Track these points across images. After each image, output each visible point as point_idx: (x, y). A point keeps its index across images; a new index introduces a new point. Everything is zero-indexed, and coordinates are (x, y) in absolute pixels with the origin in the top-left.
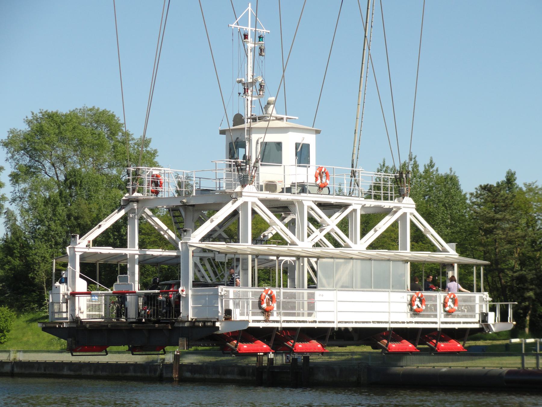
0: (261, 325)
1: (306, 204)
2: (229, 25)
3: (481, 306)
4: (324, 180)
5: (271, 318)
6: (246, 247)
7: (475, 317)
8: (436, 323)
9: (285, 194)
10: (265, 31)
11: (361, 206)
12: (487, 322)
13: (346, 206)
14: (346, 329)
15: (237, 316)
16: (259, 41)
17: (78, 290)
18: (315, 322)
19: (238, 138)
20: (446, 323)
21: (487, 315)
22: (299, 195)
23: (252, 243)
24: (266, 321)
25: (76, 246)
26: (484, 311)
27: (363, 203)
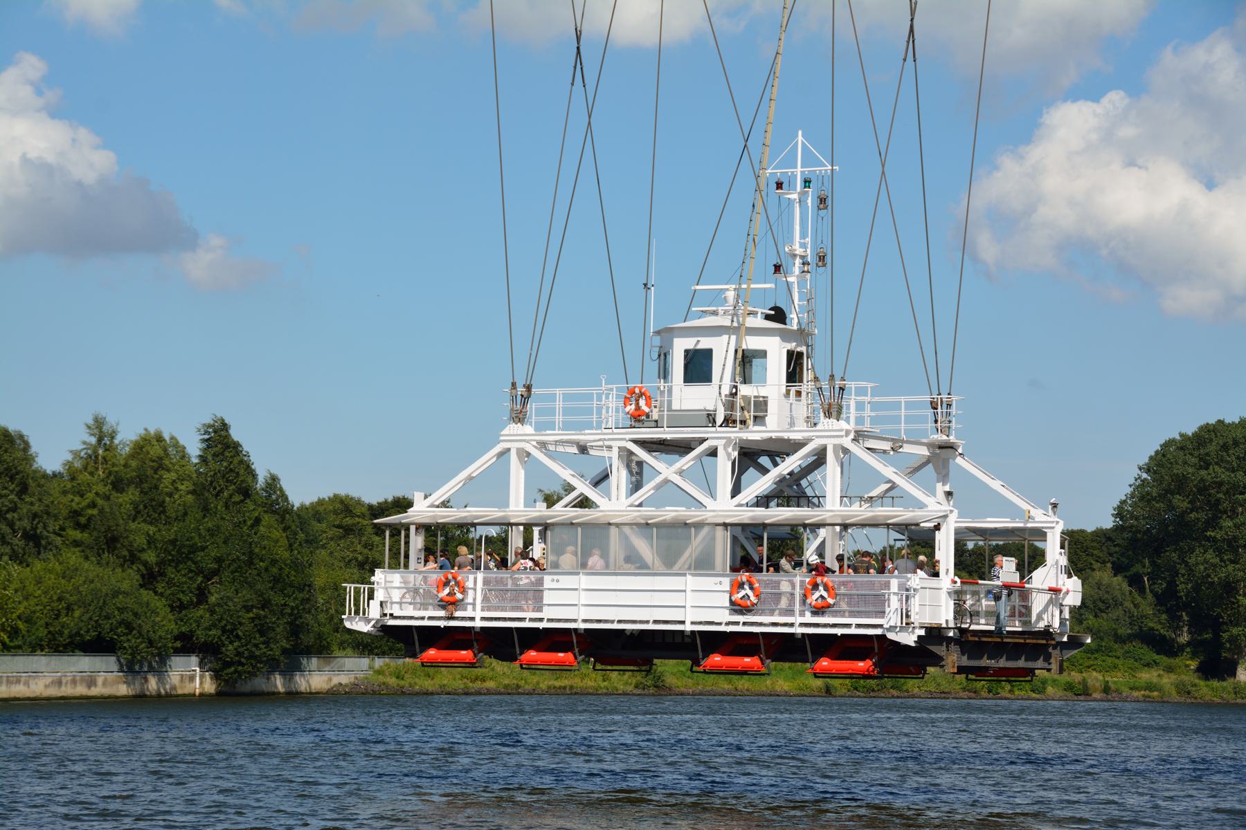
0: (442, 624)
5: (458, 614)
11: (724, 441)
18: (541, 620)
20: (817, 625)
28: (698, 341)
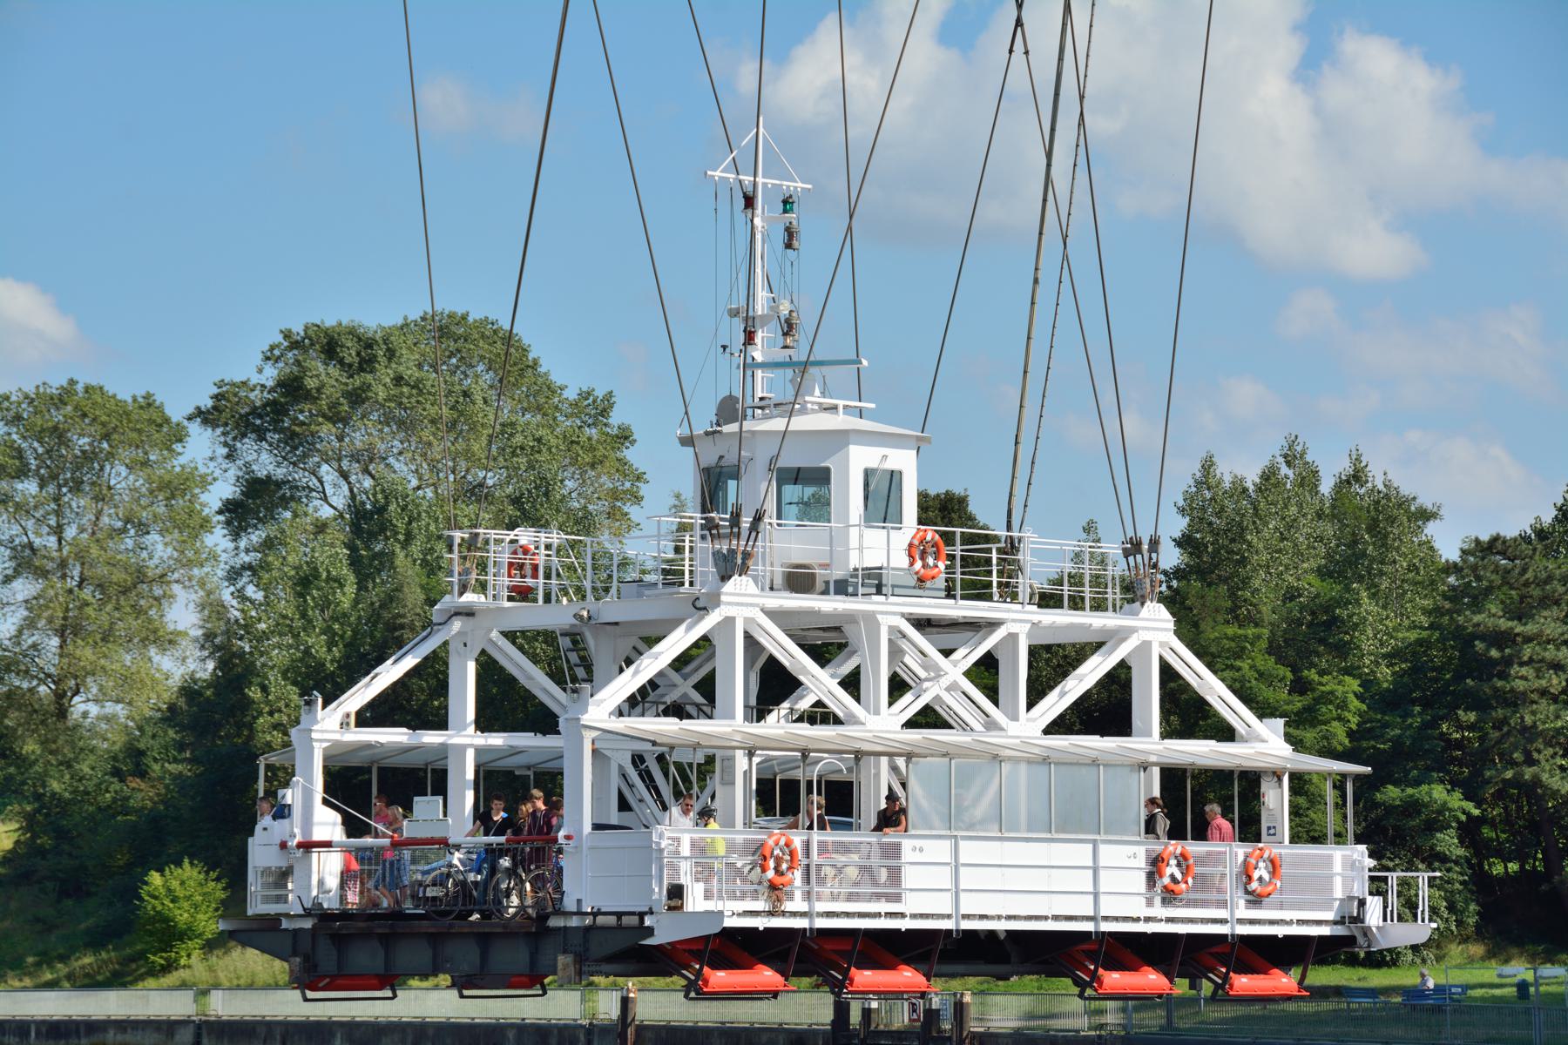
0: (760, 923)
1: (886, 622)
2: (706, 173)
3: (1347, 882)
4: (930, 561)
5: (789, 906)
6: (729, 729)
7: (1326, 906)
8: (1223, 921)
9: (832, 597)
10: (800, 184)
12: (1363, 921)
13: (993, 625)
14: (992, 934)
15: (696, 901)
16: (785, 211)
17: (318, 836)
18: (902, 915)
19: (721, 457)
20: (1252, 922)
21: (1362, 903)
22: (866, 599)
23: (746, 719)
24: (771, 914)
25: (315, 728)
26: (1357, 893)
27: (1035, 618)
28: (885, 457)
